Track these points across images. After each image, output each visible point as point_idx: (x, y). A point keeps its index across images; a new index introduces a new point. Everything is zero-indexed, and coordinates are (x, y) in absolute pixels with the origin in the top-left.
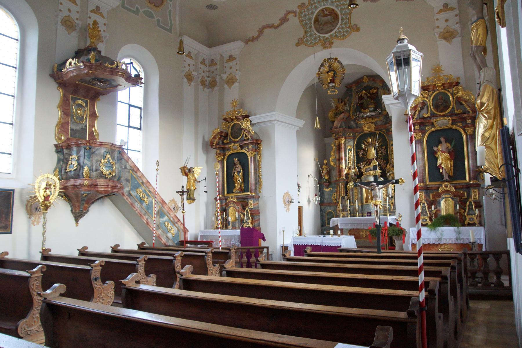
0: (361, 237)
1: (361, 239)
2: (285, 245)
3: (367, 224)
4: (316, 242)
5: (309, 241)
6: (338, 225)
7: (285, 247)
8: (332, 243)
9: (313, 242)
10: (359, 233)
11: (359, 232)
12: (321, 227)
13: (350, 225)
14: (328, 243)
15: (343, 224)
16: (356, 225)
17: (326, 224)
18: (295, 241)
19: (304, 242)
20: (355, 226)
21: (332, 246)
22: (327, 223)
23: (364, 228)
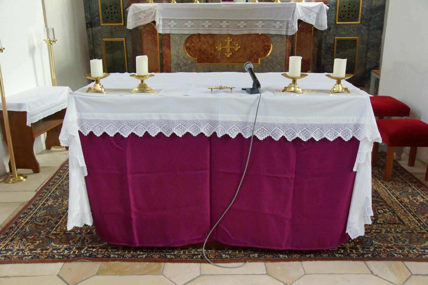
0: (219, 57)
1: (218, 61)
2: (12, 106)
3: (239, 21)
4: (213, 123)
5: (173, 117)
6: (154, 22)
7: (11, 113)
8: (306, 127)
9: (197, 124)
10: (213, 45)
11: (214, 42)
12: (87, 27)
13: (189, 24)
14: (284, 126)
15: (170, 20)
16: (207, 24)
17: (99, 20)
18: (87, 116)
19: (147, 123)
20: (204, 26)
21: (305, 139)
22: (103, 19)
23: (230, 33)
